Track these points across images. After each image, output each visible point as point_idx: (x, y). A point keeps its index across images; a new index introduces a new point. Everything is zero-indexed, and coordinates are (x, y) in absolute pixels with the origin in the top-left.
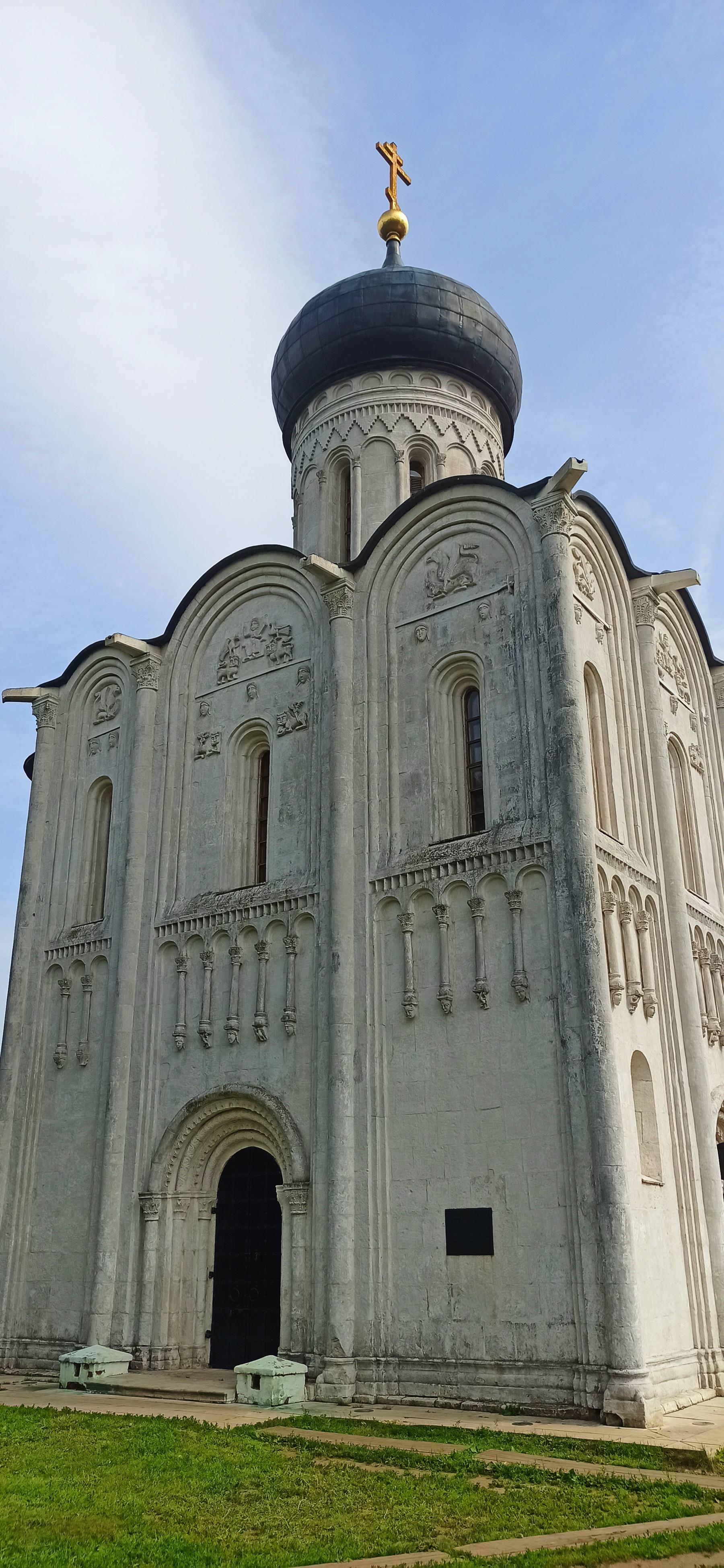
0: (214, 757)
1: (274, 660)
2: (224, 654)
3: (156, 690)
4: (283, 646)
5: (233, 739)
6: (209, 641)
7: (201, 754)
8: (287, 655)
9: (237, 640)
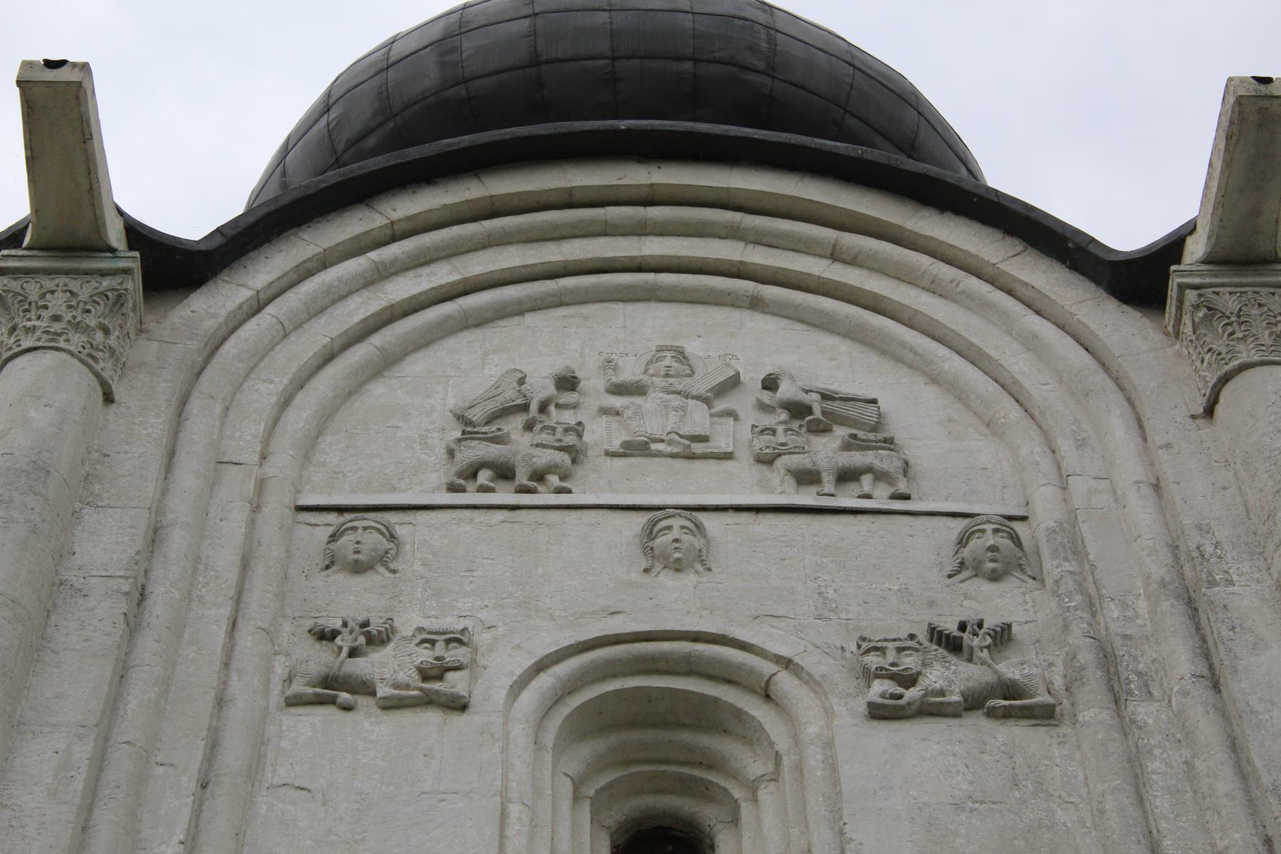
0: (432, 717)
1: (807, 477)
2: (492, 406)
3: (108, 398)
4: (847, 447)
5: (545, 681)
6: (388, 362)
7: (333, 690)
8: (881, 476)
9: (567, 382)
